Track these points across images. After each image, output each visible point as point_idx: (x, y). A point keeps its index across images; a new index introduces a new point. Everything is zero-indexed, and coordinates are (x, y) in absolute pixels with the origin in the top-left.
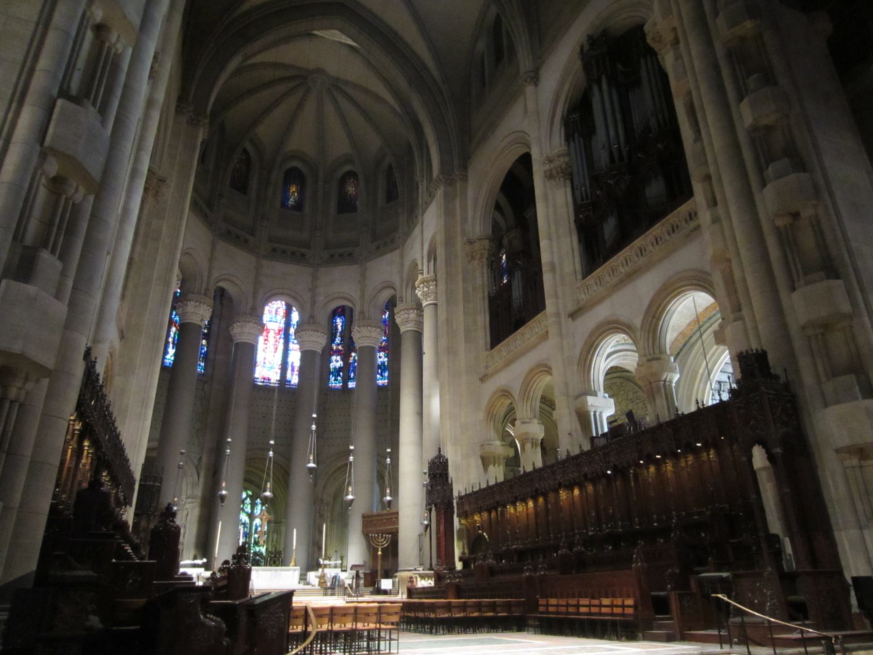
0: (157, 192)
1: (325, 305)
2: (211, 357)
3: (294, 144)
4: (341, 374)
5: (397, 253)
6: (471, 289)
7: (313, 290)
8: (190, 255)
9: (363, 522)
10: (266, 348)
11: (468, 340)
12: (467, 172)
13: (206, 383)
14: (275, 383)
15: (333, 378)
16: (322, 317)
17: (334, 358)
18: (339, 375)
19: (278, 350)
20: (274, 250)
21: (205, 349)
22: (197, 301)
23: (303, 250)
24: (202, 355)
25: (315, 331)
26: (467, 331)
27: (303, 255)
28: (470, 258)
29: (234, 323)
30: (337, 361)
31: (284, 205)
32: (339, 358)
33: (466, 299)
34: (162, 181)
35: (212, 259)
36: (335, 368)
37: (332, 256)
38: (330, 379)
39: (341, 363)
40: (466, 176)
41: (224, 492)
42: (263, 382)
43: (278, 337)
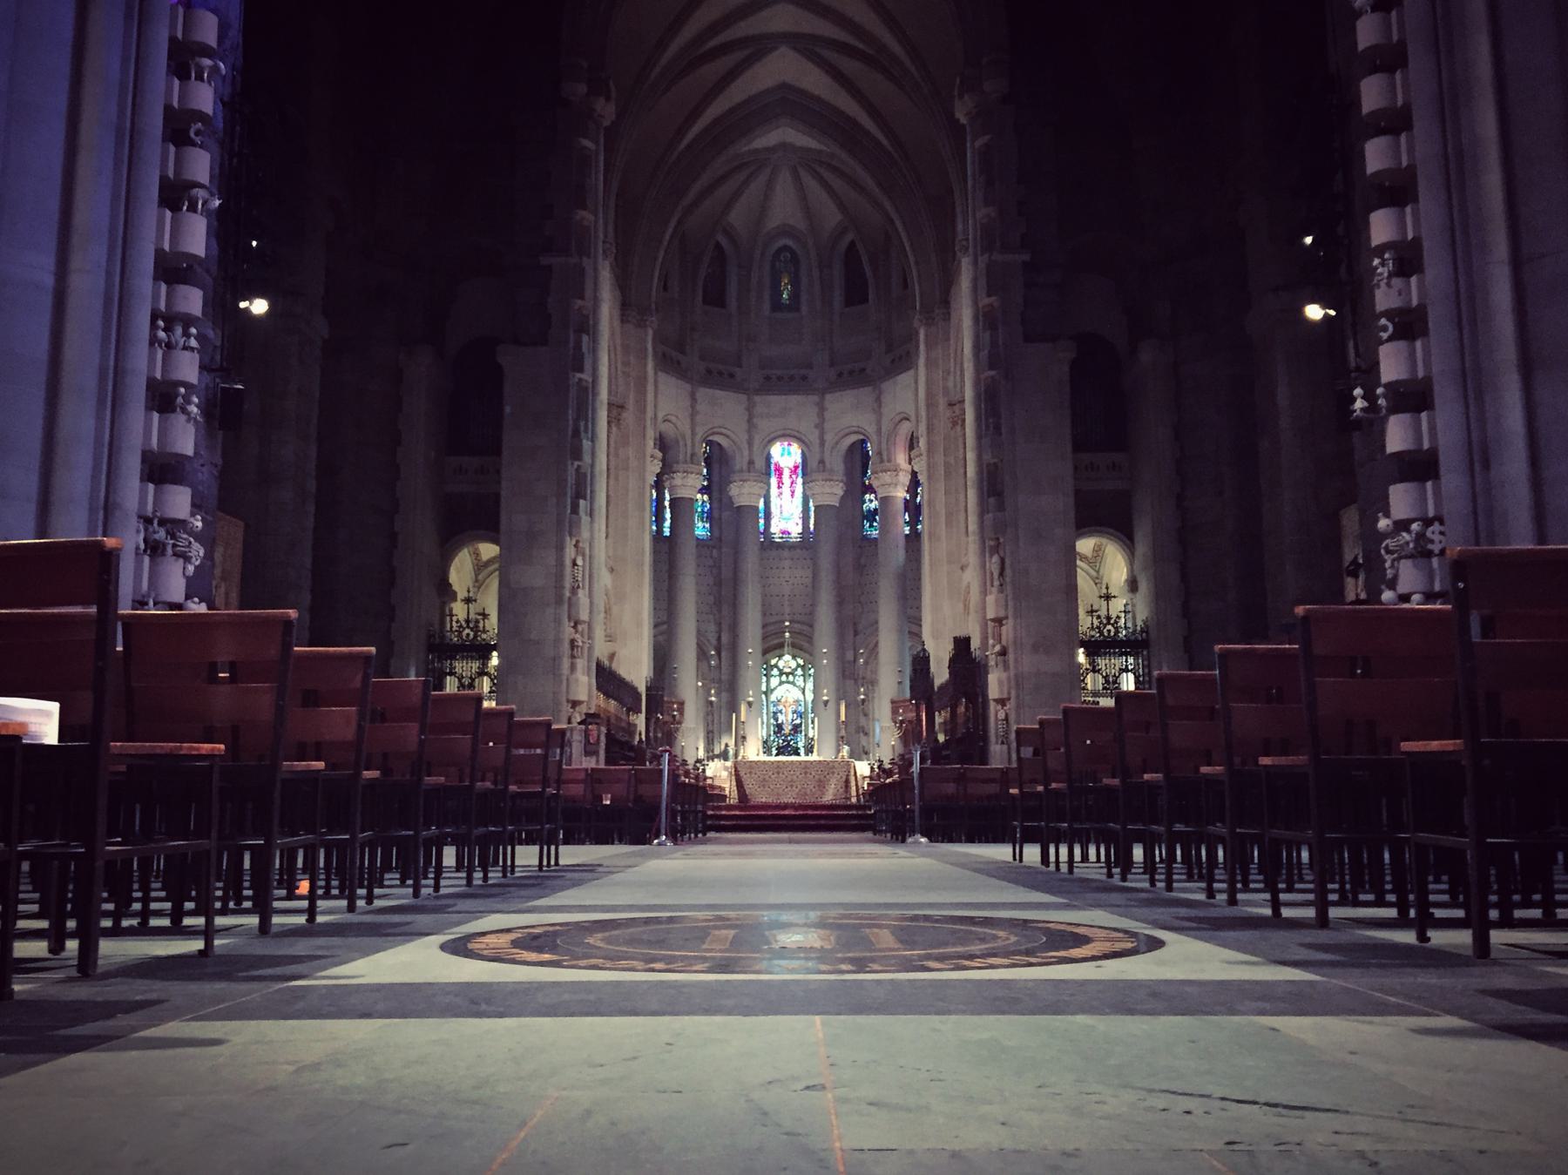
0: (619, 420)
1: (837, 443)
2: (716, 514)
3: (774, 220)
4: (877, 517)
5: (911, 372)
6: (952, 461)
7: (820, 426)
8: (669, 421)
9: (892, 708)
10: (781, 494)
11: (949, 523)
12: (949, 308)
13: (714, 547)
14: (797, 538)
15: (868, 525)
16: (837, 463)
17: (867, 497)
18: (875, 520)
19: (796, 493)
20: (768, 378)
21: (708, 506)
22: (685, 472)
23: (803, 372)
24: (706, 515)
25: (826, 480)
26: (949, 515)
27: (804, 378)
28: (951, 425)
29: (731, 483)
30: (871, 501)
31: (777, 305)
32: (873, 496)
33: (948, 474)
34: (622, 407)
35: (693, 414)
36: (869, 511)
37: (840, 375)
38: (864, 526)
39: (877, 502)
40: (949, 314)
41: (713, 699)
42: (782, 538)
43: (793, 476)
